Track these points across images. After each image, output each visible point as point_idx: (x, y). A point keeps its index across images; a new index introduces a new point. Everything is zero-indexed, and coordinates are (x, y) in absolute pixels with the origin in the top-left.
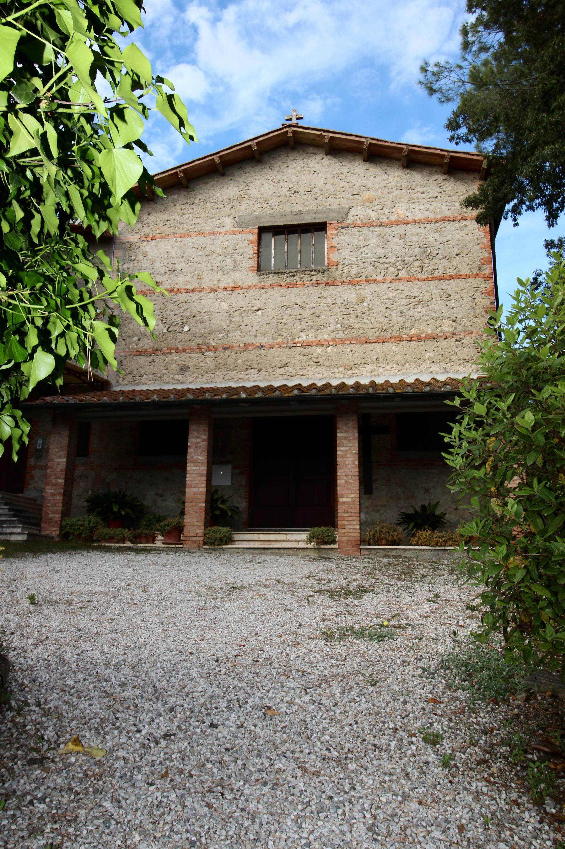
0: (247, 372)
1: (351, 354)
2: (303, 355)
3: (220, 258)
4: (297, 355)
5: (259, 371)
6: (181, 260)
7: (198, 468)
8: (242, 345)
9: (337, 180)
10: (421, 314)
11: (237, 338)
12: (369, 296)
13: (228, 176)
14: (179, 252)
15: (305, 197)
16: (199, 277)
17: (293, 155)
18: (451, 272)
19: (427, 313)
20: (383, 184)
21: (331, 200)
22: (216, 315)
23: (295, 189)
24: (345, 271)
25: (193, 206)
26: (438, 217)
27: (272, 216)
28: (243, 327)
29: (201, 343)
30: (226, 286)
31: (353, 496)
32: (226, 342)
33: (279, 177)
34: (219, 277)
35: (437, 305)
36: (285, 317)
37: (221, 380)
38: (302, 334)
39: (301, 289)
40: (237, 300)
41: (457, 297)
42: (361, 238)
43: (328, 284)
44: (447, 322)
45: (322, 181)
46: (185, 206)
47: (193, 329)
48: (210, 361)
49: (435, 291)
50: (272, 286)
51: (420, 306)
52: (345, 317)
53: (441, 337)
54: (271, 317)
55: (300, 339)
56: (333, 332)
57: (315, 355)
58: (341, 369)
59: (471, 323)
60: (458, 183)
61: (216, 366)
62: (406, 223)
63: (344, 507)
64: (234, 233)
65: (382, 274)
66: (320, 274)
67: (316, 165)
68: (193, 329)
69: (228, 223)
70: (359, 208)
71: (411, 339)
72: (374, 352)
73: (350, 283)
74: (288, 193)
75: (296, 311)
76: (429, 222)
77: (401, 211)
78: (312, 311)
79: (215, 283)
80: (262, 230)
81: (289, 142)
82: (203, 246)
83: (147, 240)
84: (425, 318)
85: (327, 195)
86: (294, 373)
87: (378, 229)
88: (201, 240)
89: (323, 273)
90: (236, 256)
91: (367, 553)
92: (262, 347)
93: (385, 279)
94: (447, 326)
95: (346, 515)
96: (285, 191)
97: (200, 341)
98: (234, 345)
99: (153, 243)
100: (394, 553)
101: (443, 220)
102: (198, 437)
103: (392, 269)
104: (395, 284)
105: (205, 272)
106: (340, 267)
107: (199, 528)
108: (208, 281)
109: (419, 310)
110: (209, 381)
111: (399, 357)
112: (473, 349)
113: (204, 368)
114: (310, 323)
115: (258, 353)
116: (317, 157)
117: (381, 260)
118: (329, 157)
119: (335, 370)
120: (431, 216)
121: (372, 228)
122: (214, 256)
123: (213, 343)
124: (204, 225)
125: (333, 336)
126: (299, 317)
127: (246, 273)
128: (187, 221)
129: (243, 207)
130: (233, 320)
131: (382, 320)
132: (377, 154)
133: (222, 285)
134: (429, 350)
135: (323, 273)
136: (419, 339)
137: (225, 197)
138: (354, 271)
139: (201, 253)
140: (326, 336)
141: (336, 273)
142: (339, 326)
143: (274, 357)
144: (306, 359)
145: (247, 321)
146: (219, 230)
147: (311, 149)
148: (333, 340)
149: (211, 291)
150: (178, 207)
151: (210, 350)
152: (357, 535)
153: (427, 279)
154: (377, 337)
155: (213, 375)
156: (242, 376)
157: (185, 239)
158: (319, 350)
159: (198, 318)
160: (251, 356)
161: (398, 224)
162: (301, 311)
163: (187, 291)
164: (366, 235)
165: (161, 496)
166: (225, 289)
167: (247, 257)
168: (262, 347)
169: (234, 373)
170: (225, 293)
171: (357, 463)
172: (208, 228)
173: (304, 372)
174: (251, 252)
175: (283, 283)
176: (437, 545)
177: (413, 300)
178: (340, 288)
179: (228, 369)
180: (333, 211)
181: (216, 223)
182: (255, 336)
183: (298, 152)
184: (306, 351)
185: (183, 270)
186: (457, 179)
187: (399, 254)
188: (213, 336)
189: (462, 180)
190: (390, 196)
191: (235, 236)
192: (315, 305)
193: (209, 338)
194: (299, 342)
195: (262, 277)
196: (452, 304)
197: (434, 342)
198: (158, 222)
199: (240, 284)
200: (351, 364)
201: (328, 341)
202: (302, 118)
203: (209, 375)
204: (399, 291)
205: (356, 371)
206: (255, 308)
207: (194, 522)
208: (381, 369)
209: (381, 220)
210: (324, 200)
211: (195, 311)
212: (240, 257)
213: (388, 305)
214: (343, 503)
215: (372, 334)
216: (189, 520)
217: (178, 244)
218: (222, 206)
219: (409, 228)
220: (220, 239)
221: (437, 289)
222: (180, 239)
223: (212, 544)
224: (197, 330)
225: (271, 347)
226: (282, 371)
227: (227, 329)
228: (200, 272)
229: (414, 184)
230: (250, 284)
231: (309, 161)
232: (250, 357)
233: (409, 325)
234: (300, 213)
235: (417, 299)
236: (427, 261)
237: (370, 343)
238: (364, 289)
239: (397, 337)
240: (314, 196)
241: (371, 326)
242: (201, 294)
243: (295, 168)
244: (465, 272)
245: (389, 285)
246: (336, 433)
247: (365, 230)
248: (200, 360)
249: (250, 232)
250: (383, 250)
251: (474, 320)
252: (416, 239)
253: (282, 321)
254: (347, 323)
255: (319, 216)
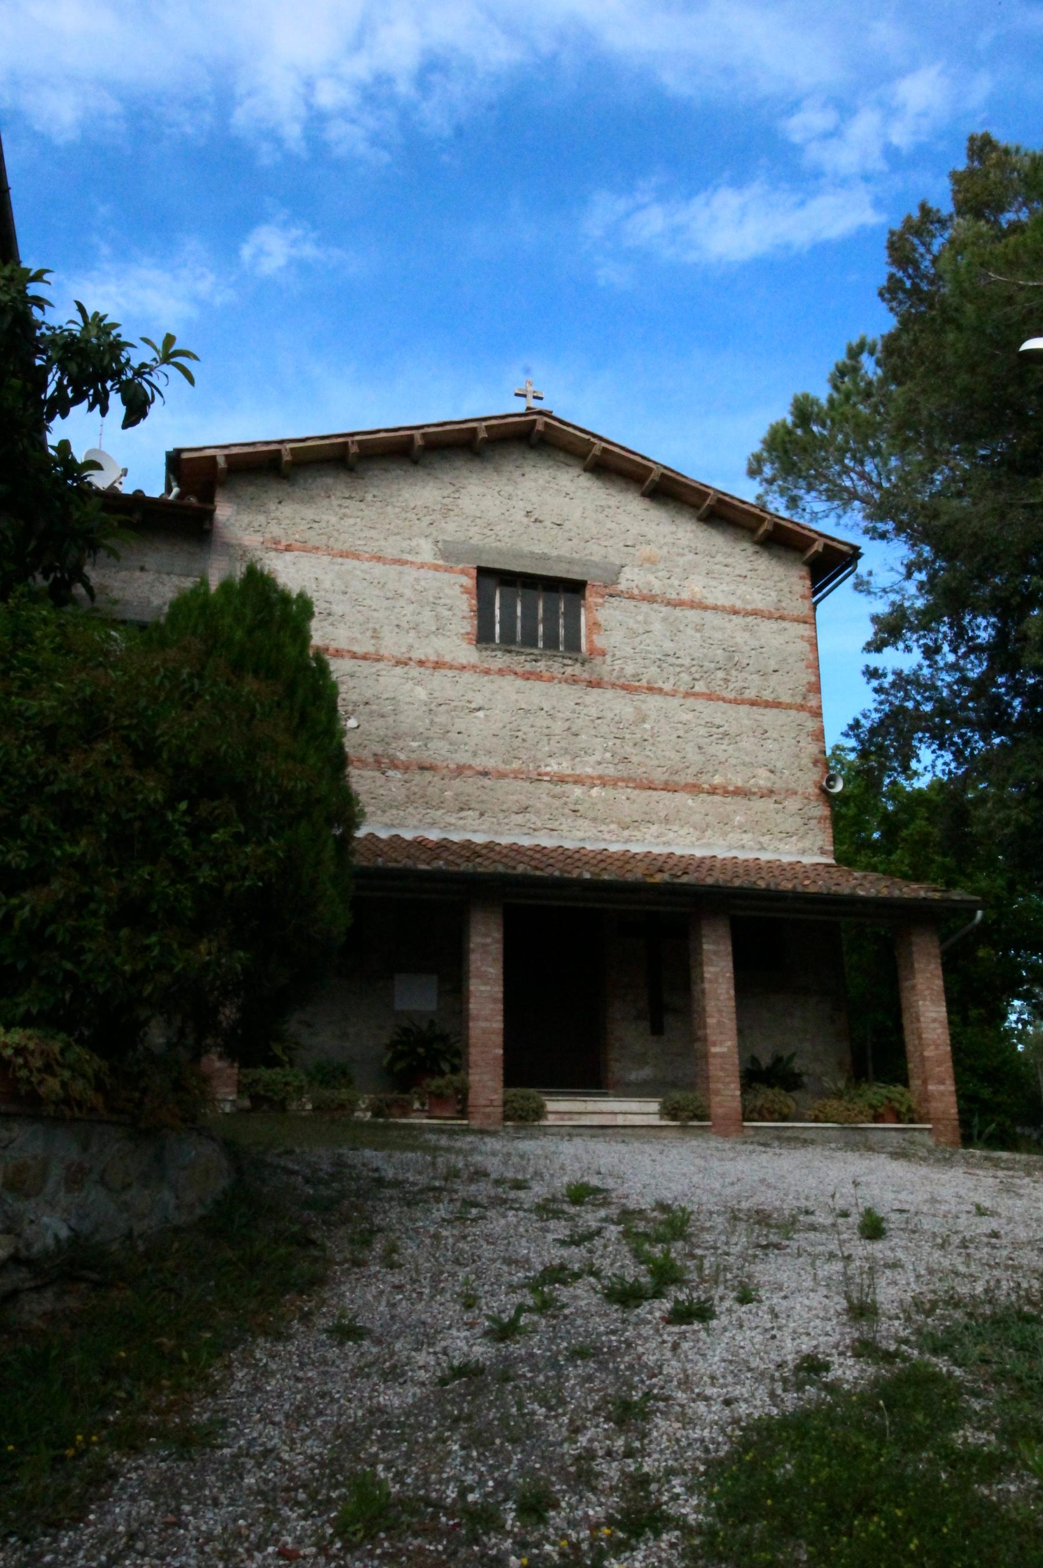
0: (463, 814)
1: (627, 803)
2: (554, 797)
3: (412, 607)
4: (544, 796)
5: (482, 814)
6: (341, 597)
7: (488, 988)
8: (452, 766)
9: (601, 516)
10: (727, 755)
11: (443, 752)
12: (653, 715)
13: (425, 467)
14: (338, 583)
15: (554, 532)
16: (376, 635)
17: (532, 456)
18: (767, 696)
19: (736, 754)
20: (670, 539)
21: (592, 547)
22: (406, 707)
23: (536, 515)
24: (617, 667)
25: (362, 505)
26: (749, 607)
27: (500, 552)
28: (453, 735)
29: (380, 752)
30: (423, 658)
31: (729, 1043)
32: (426, 757)
33: (509, 489)
34: (410, 640)
35: (747, 743)
36: (524, 729)
37: (416, 823)
38: (552, 761)
39: (548, 684)
40: (441, 683)
41: (775, 735)
42: (640, 618)
43: (590, 684)
44: (763, 773)
45: (578, 513)
46: (347, 502)
47: (365, 726)
48: (398, 789)
49: (746, 722)
50: (501, 672)
51: (726, 741)
52: (618, 741)
53: (754, 794)
54: (501, 725)
55: (548, 769)
56: (600, 763)
57: (573, 798)
58: (613, 827)
59: (794, 778)
60: (773, 562)
61: (408, 797)
62: (706, 608)
63: (718, 1061)
64: (436, 568)
65: (672, 681)
66: (578, 665)
67: (568, 484)
68: (365, 726)
69: (426, 551)
70: (636, 570)
71: (713, 791)
72: (661, 805)
73: (624, 687)
74: (525, 520)
75: (542, 721)
76: (736, 612)
77: (696, 587)
78: (567, 724)
79: (404, 650)
80: (484, 573)
81: (531, 438)
82: (382, 581)
83: (276, 550)
84: (733, 761)
85: (587, 536)
86: (539, 824)
87: (664, 609)
88: (378, 569)
89: (583, 664)
90: (440, 609)
91: (752, 1133)
92: (485, 774)
93: (676, 691)
94: (763, 779)
95: (721, 1074)
96: (519, 515)
97: (379, 749)
98: (439, 764)
99: (288, 556)
100: (788, 1134)
101: (755, 613)
102: (486, 935)
103: (685, 677)
104: (690, 702)
105: (386, 628)
106: (608, 659)
107: (495, 1092)
108: (392, 644)
109: (724, 747)
110: (396, 822)
111: (697, 818)
112: (798, 819)
113: (386, 799)
114: (563, 744)
115: (480, 784)
116: (571, 470)
117: (671, 660)
118: (588, 475)
119: (603, 828)
120: (739, 605)
121: (655, 606)
122: (402, 602)
123: (402, 757)
124: (383, 543)
125: (600, 770)
126: (547, 731)
127: (458, 642)
128: (352, 530)
129: (451, 527)
130: (437, 720)
131: (672, 754)
132: (668, 491)
133: (417, 655)
134: (739, 811)
135: (583, 664)
136: (726, 792)
137: (419, 503)
138: (630, 670)
139: (377, 592)
140: (589, 770)
141: (605, 668)
142: (608, 755)
143: (507, 793)
144: (557, 803)
145: (460, 724)
146: (410, 558)
147: (561, 456)
148: (600, 777)
149: (398, 663)
150: (335, 502)
151: (396, 767)
152: (736, 1105)
153: (735, 702)
154: (666, 783)
155: (402, 813)
156: (453, 821)
157: (348, 560)
158: (578, 791)
159: (374, 707)
160: (467, 786)
161: (692, 607)
162: (548, 722)
163: (354, 656)
164: (647, 614)
165: (309, 1025)
166: (421, 663)
167: (460, 614)
168: (485, 774)
169: (440, 812)
170: (422, 670)
171: (732, 992)
172: (391, 548)
173: (555, 825)
174: (465, 607)
175: (519, 669)
176: (846, 1121)
177: (714, 730)
178: (610, 693)
179: (428, 805)
180: (596, 565)
181: (405, 544)
182: (475, 754)
183: (540, 455)
184: (558, 789)
185: (347, 618)
186: (773, 556)
187: (696, 655)
188: (401, 743)
189: (779, 558)
190: (681, 561)
191: (437, 574)
192: (571, 716)
193: (394, 745)
194: (547, 774)
195: (484, 653)
196: (770, 745)
197: (745, 801)
198: (298, 520)
199: (448, 658)
200: (628, 820)
201: (592, 778)
202: (541, 399)
203: (394, 812)
204: (696, 714)
205: (636, 833)
206: (473, 706)
207: (726, 1092)
208: (671, 835)
209: (668, 596)
210: (583, 544)
211: (368, 694)
212: (447, 613)
213: (681, 733)
214: (715, 1055)
215: (659, 776)
216: (477, 1078)
217: (337, 568)
218: (414, 517)
219: (709, 615)
220: (411, 574)
221: (749, 719)
222: (340, 560)
223: (521, 1118)
224: (373, 730)
225: (502, 776)
226: (519, 819)
227: (426, 734)
228: (377, 626)
229: (714, 549)
230: (465, 662)
231: (559, 474)
232: (468, 789)
233: (710, 768)
234: (545, 558)
235: (721, 730)
236: (734, 673)
237: (655, 789)
238: (644, 702)
239: (694, 786)
240: (567, 535)
241: (656, 763)
242: (380, 665)
243: (535, 481)
244: (786, 699)
245: (682, 701)
246: (701, 944)
247: (645, 607)
248: (378, 783)
249: (463, 572)
250: (672, 644)
251: (799, 774)
252: (718, 635)
253: (519, 734)
254: (622, 752)
255: (576, 569)
